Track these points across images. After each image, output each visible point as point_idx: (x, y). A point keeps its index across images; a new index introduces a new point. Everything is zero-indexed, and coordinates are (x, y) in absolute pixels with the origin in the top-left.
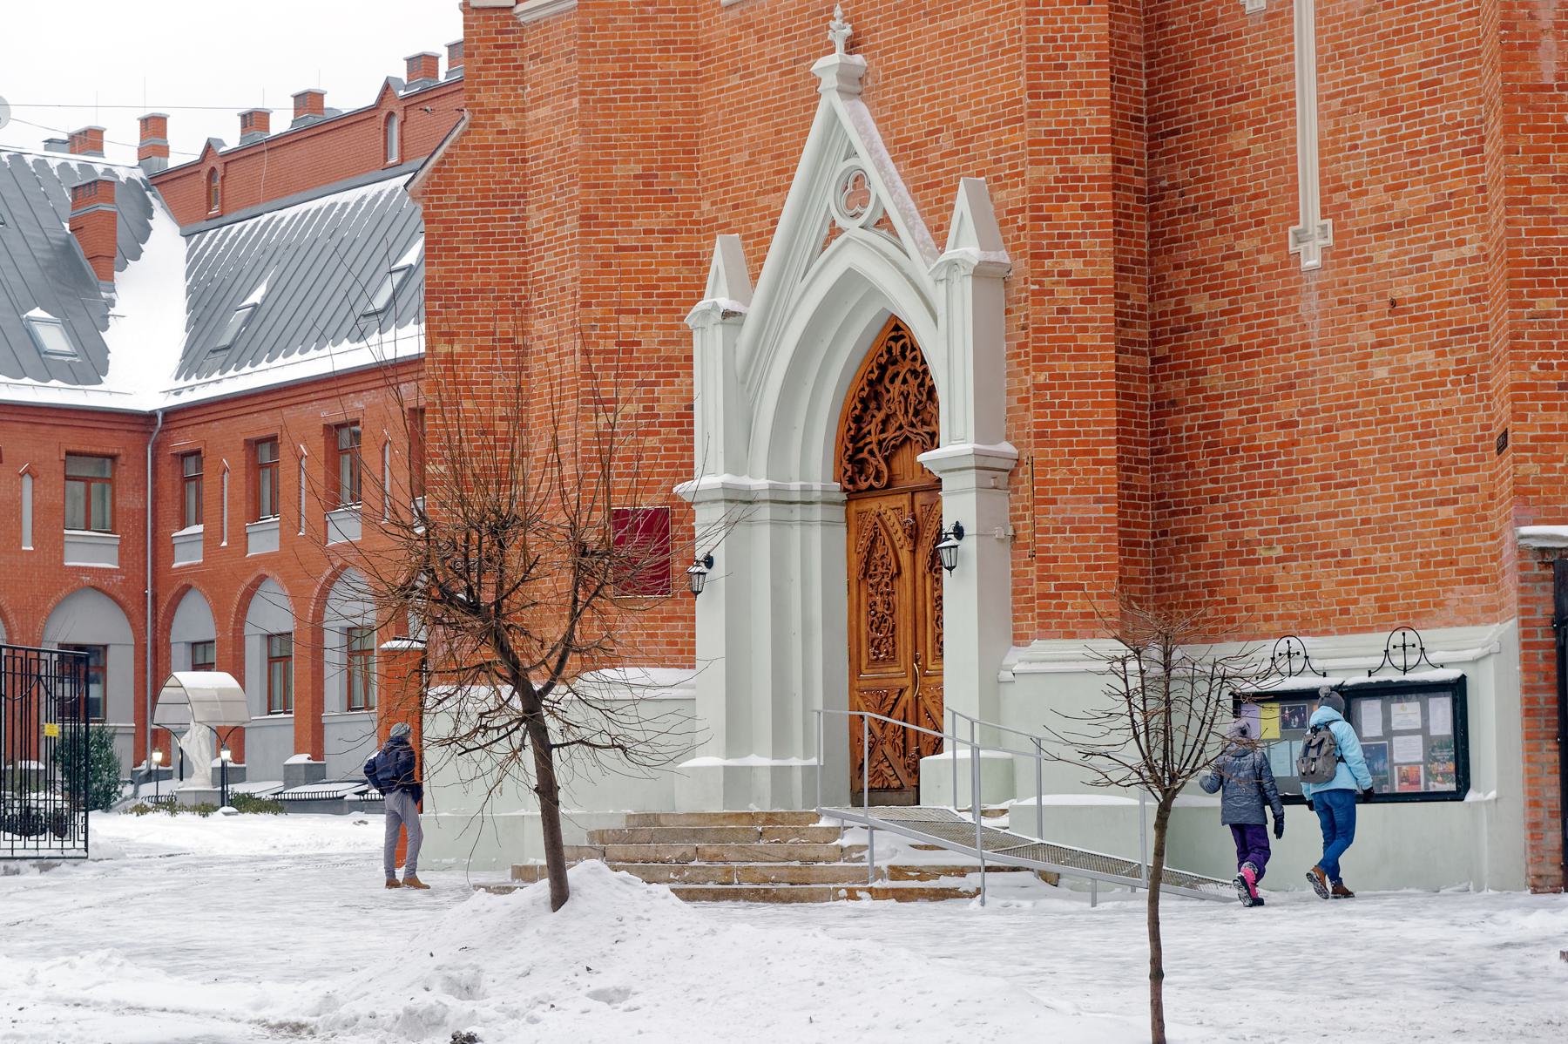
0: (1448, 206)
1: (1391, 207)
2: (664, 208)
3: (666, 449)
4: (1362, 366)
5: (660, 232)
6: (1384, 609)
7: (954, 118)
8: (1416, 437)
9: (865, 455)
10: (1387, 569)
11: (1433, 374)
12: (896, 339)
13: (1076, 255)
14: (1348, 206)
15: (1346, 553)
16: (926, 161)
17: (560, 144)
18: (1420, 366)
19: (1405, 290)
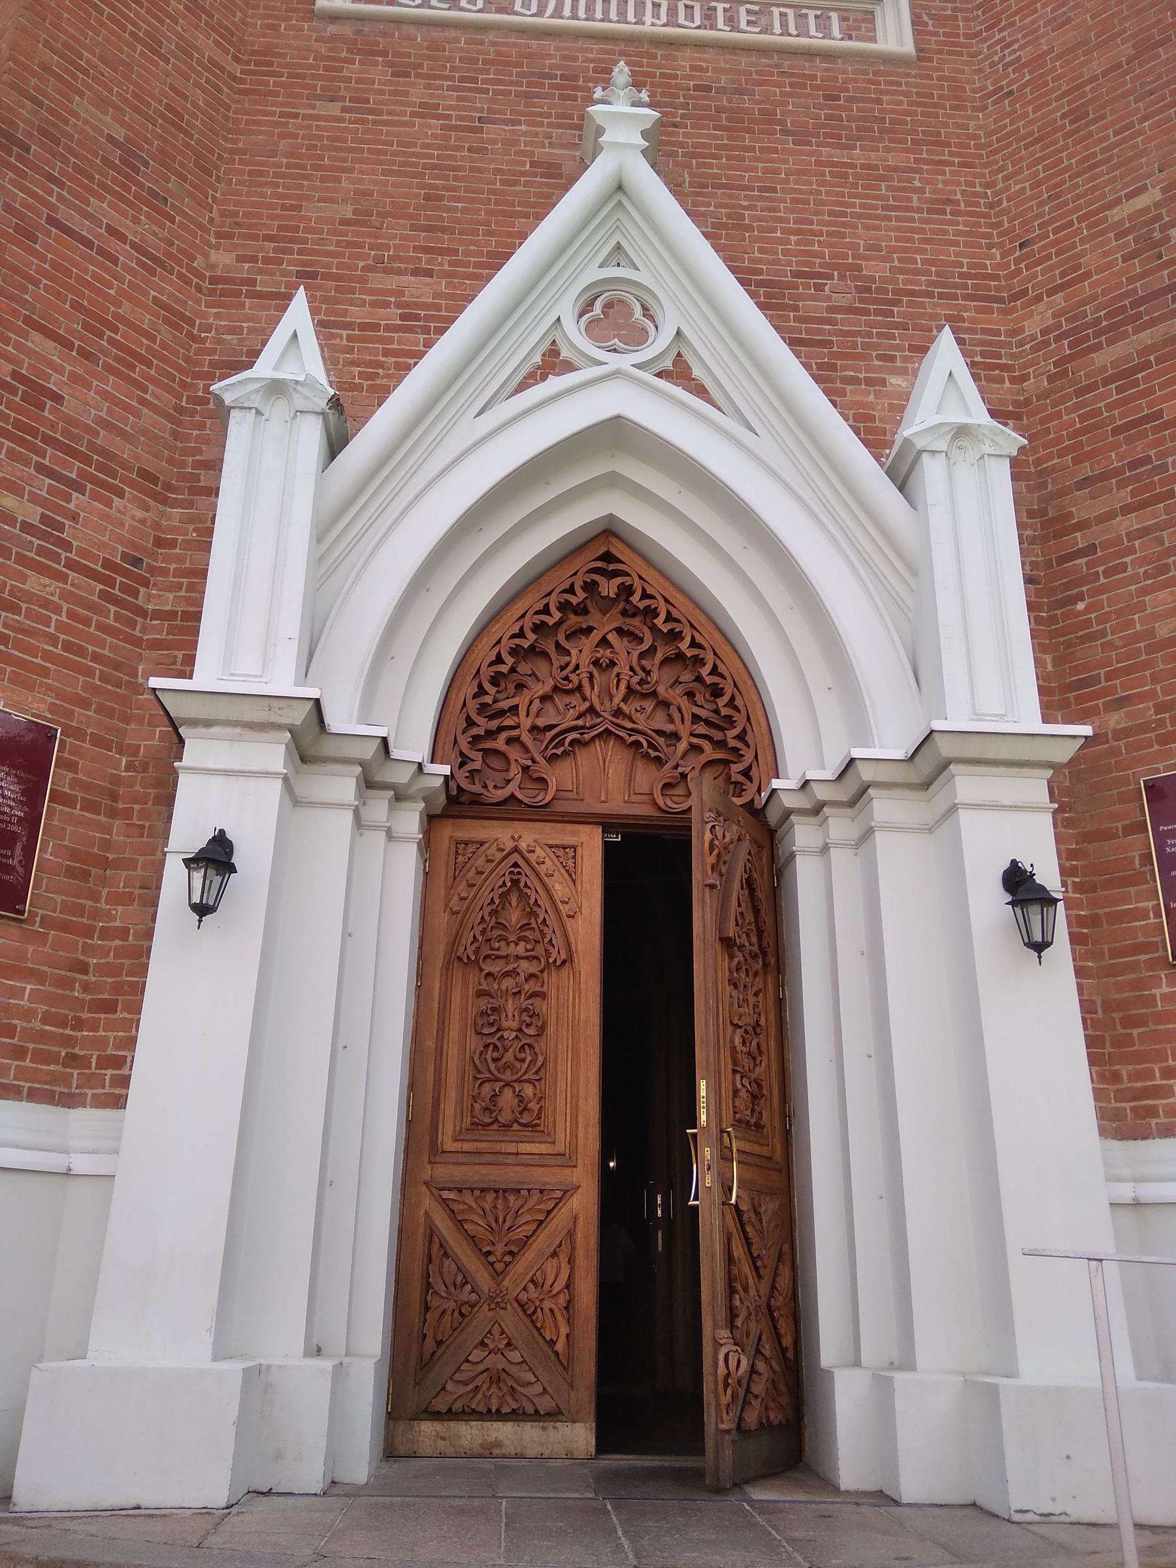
2: (148, 216)
3: (71, 614)
5: (134, 246)
7: (859, 268)
9: (500, 743)
16: (796, 309)
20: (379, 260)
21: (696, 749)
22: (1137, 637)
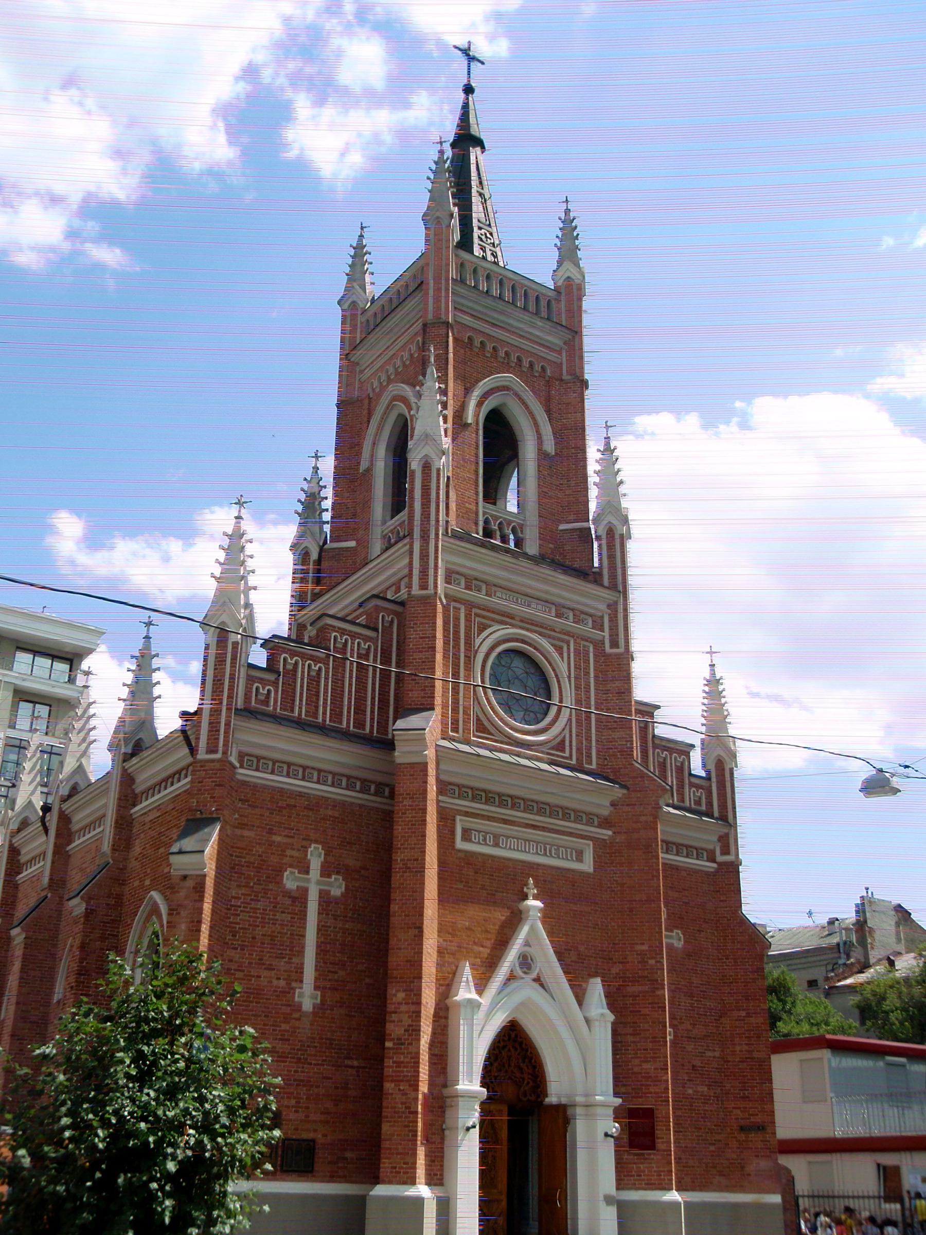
0: (709, 1036)
1: (691, 1031)
4: (684, 1087)
6: (693, 1182)
8: (702, 1118)
12: (513, 1030)
14: (677, 1026)
17: (260, 856)
18: (703, 1092)
19: (698, 1063)
20: (474, 942)
21: (528, 1083)
22: (629, 1069)
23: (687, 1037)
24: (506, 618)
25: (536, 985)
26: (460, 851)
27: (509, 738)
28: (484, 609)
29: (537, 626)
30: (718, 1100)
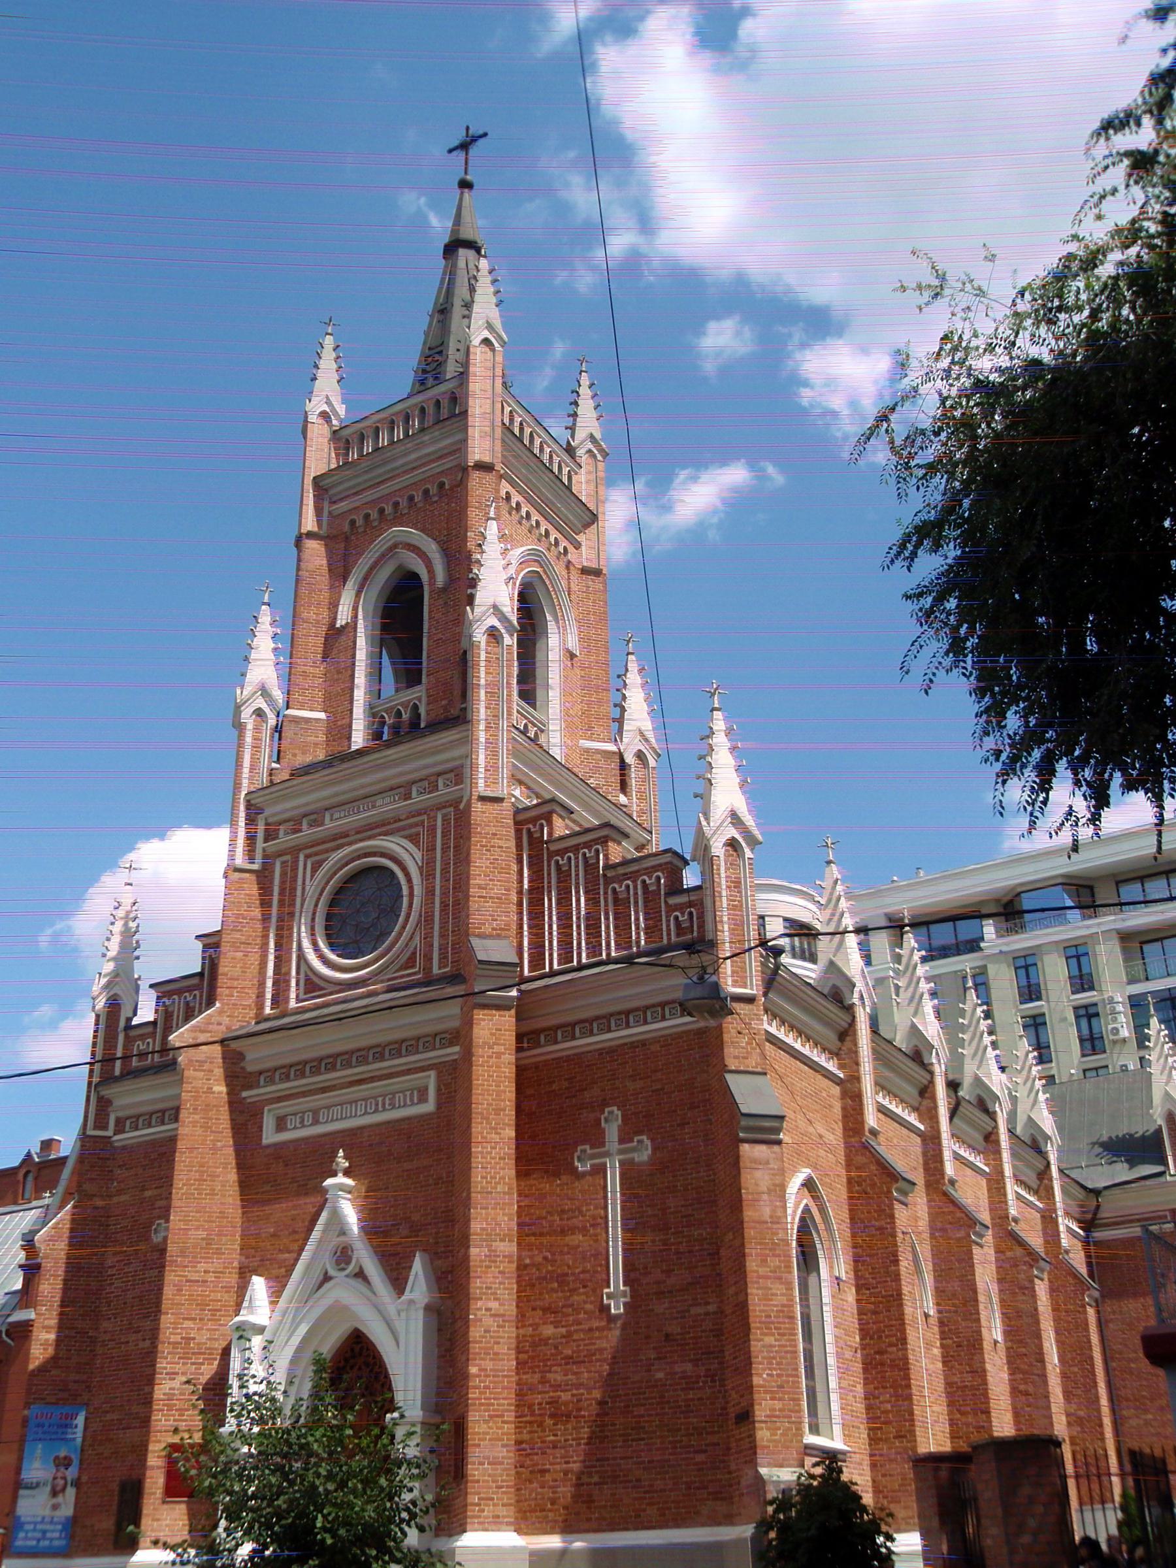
1: (665, 1282)
8: (682, 1412)
10: (665, 1490)
11: (691, 1377)
12: (358, 1343)
13: (495, 1299)
15: (638, 1480)
19: (674, 1328)
23: (656, 1293)
24: (340, 838)
25: (357, 1284)
26: (268, 1146)
27: (340, 984)
28: (312, 846)
29: (377, 827)
30: (713, 1381)
